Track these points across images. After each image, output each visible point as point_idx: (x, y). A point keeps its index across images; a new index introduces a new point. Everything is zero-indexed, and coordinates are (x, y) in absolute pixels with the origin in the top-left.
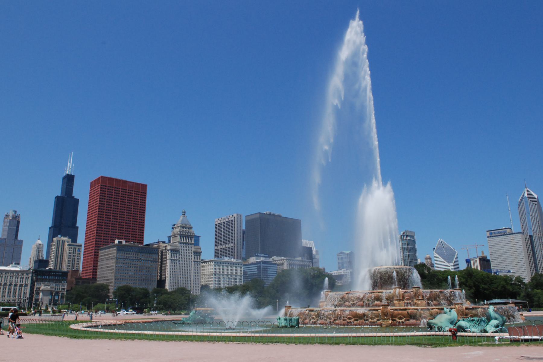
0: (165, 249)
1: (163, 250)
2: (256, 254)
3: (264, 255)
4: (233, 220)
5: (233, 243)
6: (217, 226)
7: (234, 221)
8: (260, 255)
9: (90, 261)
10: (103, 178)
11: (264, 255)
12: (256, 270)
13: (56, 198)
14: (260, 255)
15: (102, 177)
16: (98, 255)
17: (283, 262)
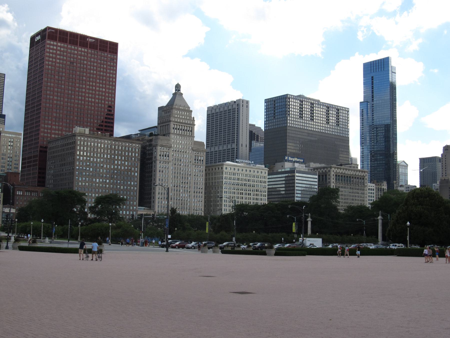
0: (150, 145)
1: (146, 146)
2: (286, 158)
3: (298, 160)
4: (235, 109)
5: (236, 143)
6: (210, 117)
7: (236, 110)
8: (291, 159)
9: (34, 161)
10: (50, 30)
11: (298, 160)
12: (284, 182)
14: (291, 159)
15: (49, 28)
16: (46, 152)
17: (326, 171)
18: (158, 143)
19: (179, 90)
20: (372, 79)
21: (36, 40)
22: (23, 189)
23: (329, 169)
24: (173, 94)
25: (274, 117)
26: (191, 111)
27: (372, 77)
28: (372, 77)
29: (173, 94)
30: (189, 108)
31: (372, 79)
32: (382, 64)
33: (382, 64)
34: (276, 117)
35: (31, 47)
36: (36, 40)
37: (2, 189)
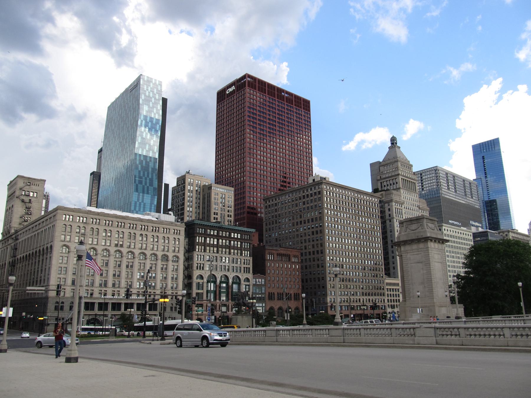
13: (91, 174)
18: (393, 199)
19: (396, 143)
20: (483, 159)
21: (227, 93)
22: (274, 252)
23: (507, 233)
24: (389, 148)
25: (423, 189)
26: (412, 166)
27: (483, 157)
28: (483, 157)
29: (389, 148)
30: (409, 161)
31: (483, 159)
32: (492, 144)
33: (492, 144)
34: (425, 189)
35: (220, 101)
36: (227, 93)
37: (251, 252)
